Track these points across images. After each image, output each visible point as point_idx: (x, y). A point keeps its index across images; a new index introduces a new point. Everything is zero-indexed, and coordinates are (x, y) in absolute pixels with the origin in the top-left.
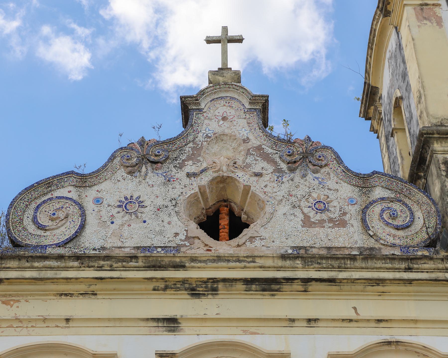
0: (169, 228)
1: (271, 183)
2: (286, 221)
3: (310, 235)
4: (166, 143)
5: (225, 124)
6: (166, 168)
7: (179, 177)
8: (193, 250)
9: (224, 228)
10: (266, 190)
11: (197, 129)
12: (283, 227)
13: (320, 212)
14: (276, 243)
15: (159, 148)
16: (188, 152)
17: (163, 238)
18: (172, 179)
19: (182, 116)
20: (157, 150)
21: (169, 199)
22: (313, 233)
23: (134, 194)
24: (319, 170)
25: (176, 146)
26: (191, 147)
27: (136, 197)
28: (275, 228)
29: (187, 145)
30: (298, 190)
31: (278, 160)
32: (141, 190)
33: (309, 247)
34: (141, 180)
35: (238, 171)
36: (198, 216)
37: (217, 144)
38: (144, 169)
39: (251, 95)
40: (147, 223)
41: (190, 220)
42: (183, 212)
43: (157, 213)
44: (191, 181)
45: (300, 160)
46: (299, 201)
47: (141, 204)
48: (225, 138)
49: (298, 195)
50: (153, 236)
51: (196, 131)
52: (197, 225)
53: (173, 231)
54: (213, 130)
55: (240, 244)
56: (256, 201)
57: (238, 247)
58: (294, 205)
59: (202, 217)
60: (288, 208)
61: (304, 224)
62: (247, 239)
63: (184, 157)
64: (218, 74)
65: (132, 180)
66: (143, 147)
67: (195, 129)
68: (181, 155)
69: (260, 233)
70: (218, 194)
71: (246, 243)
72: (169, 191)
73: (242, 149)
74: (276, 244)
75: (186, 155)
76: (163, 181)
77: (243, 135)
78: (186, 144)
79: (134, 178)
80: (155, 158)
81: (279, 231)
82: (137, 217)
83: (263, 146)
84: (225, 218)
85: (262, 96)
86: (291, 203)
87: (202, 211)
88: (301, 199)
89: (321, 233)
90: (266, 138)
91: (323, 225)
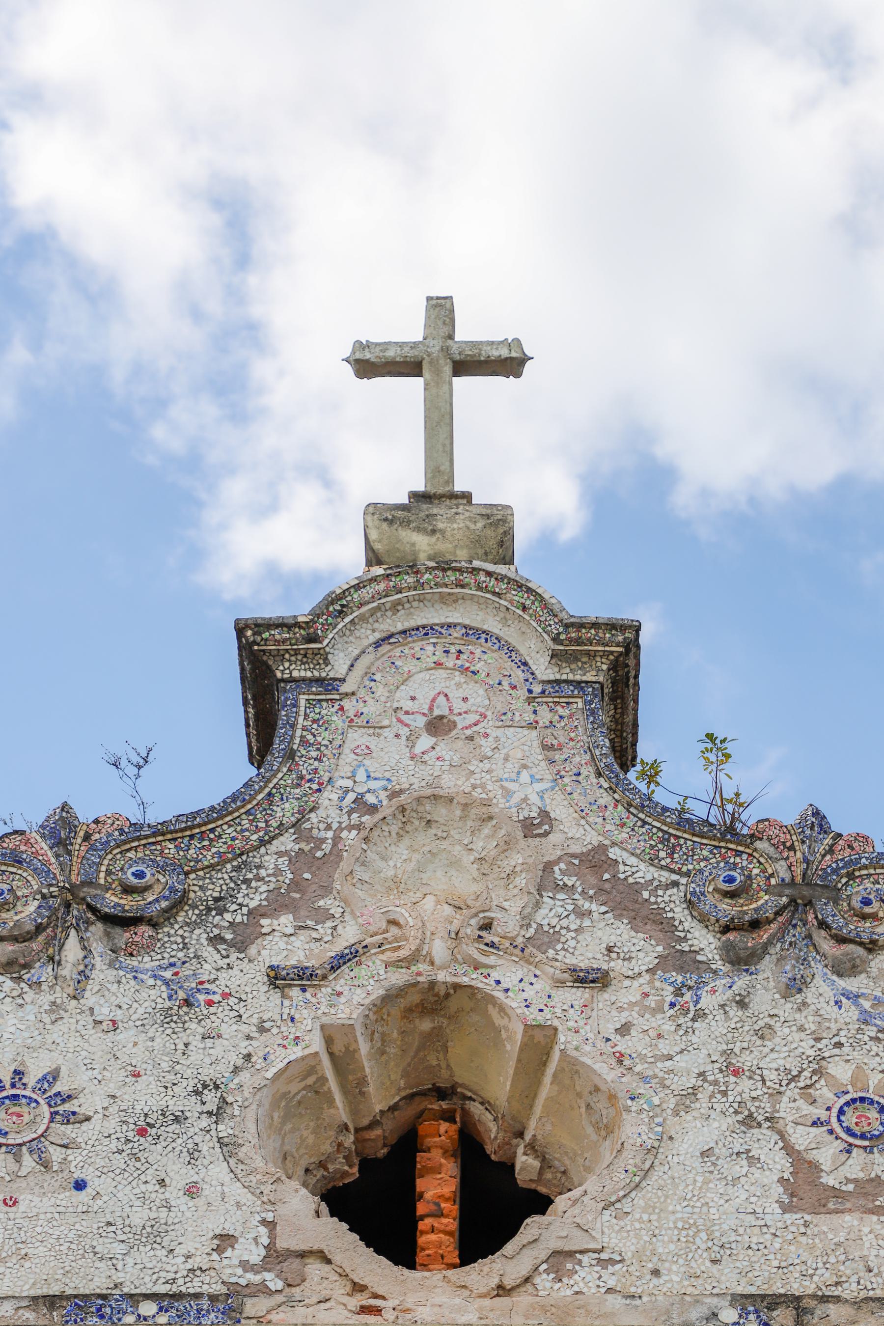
0: (188, 1214)
1: (647, 1016)
2: (711, 1185)
3: (820, 1246)
4: (171, 832)
5: (443, 749)
6: (175, 946)
7: (234, 988)
8: (300, 1310)
9: (440, 1214)
10: (623, 1045)
11: (316, 771)
12: (697, 1210)
13: (865, 1148)
14: (667, 1278)
15: (140, 855)
16: (274, 875)
17: (164, 1259)
18: (201, 997)
19: (246, 712)
20: (131, 867)
21: (192, 1083)
22: (830, 1236)
23: (29, 1062)
24: (864, 962)
25: (220, 847)
26: (286, 853)
27: (40, 1076)
28: (662, 1215)
29: (269, 842)
30: (766, 1050)
31: (680, 913)
32: (62, 1045)
33: (814, 1296)
34: (59, 1001)
35: (500, 962)
36: (323, 1158)
37: (406, 841)
38: (72, 950)
39: (561, 621)
40: (89, 1190)
41: (284, 1178)
42: (255, 1141)
43: (136, 1145)
44: (287, 1003)
45: (778, 914)
46: (771, 1095)
47: (60, 1109)
48: (440, 813)
49: (765, 1072)
50: (120, 1249)
51: (309, 781)
52: (317, 1199)
53: (211, 1227)
54: (387, 775)
55: (508, 1283)
56: (579, 1095)
57: (498, 1295)
58: (750, 1115)
59: (339, 1165)
60: (724, 1128)
61: (792, 1195)
62: (539, 1261)
63: (257, 897)
64: (409, 522)
65: (21, 1001)
66: (69, 853)
67: (304, 772)
68: (244, 887)
69: (598, 1236)
70: (409, 1065)
71: (537, 1280)
72: (190, 1047)
73: (520, 861)
74: (669, 1285)
75: (264, 888)
76: (159, 1006)
77: (525, 800)
78: (266, 838)
79: (26, 988)
80: (122, 902)
81: (684, 1229)
82: (46, 1165)
83: (614, 853)
84: (444, 1169)
85: (613, 626)
86: (736, 1105)
87: (341, 1138)
88: (782, 1089)
89: (869, 1239)
90: (625, 814)
91: (874, 1201)
